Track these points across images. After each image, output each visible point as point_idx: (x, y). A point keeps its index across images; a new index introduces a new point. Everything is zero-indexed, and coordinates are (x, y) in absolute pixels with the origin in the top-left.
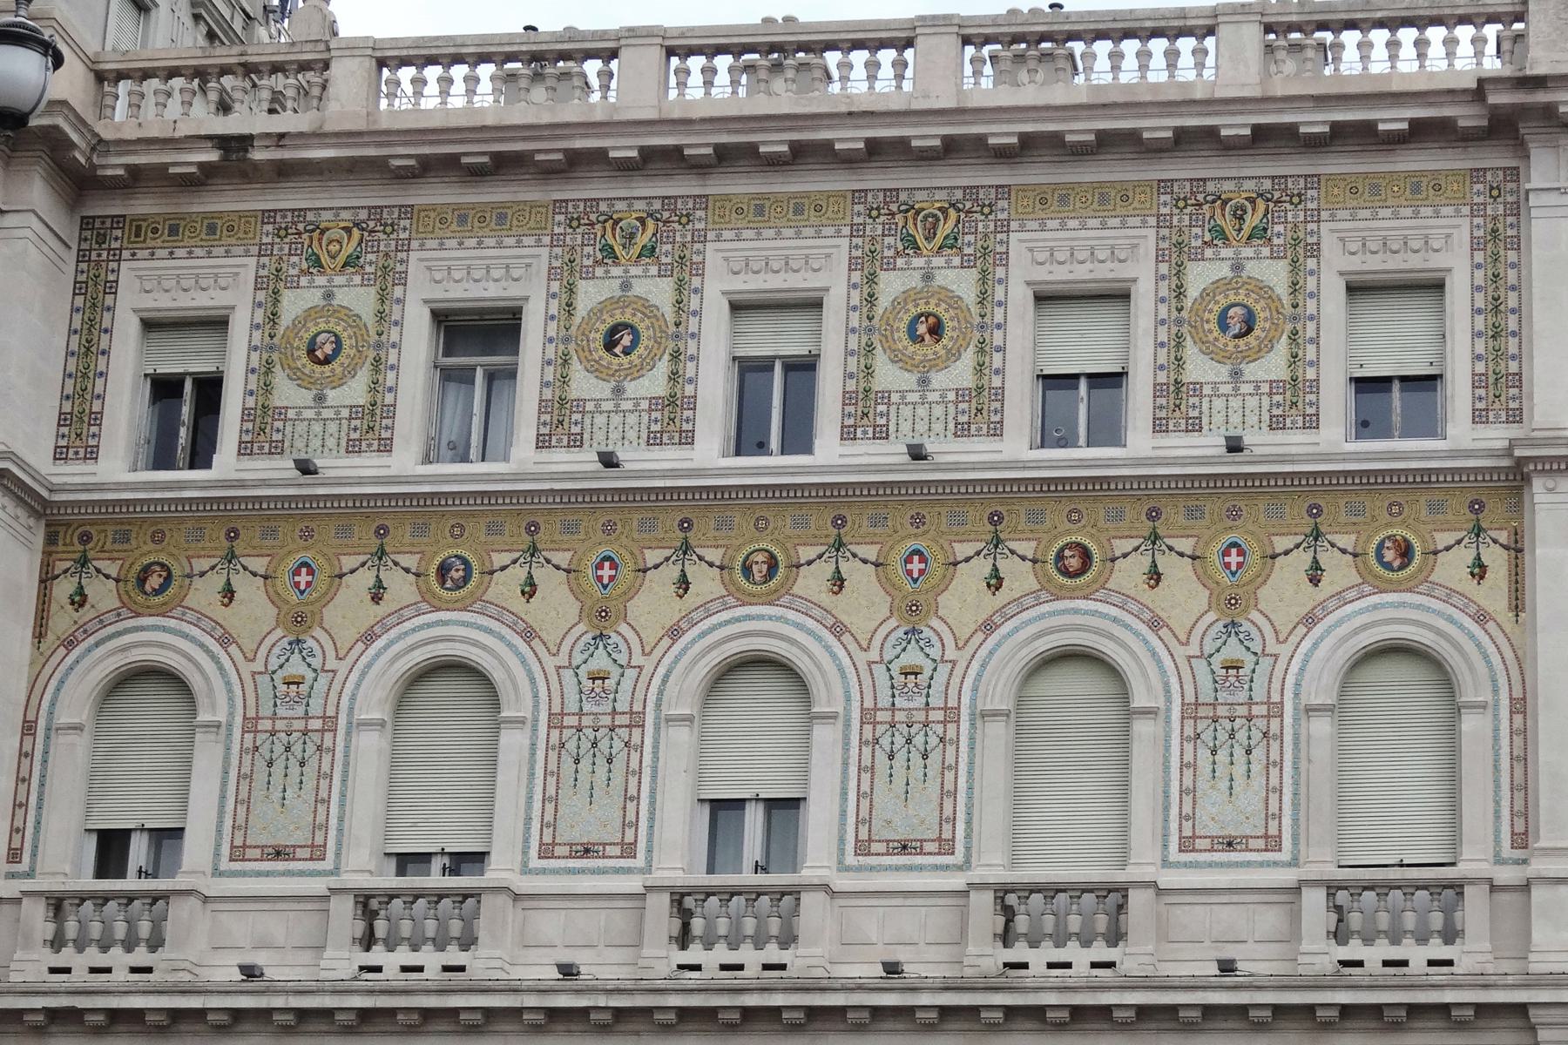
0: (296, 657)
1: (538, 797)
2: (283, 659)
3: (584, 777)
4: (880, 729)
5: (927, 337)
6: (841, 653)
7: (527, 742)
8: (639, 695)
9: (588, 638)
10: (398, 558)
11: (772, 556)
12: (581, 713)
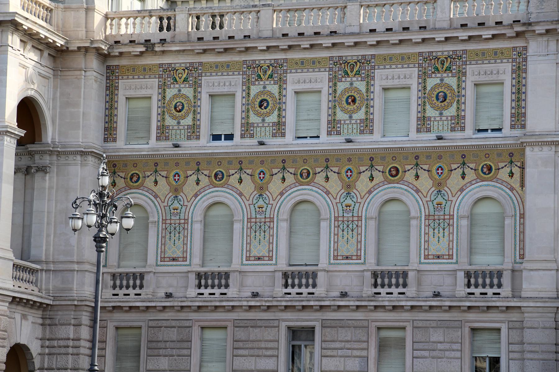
7: (241, 227)
8: (272, 213)
10: (203, 171)
12: (256, 218)
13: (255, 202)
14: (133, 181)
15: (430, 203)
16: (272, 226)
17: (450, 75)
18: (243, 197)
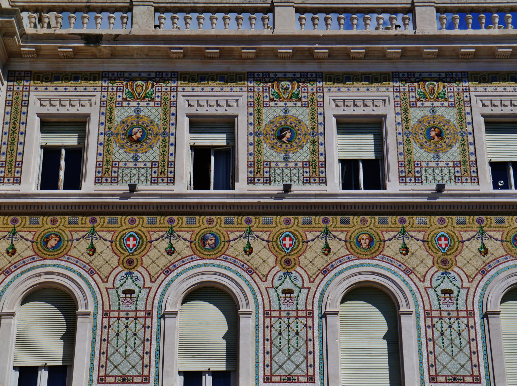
0: (129, 281)
1: (261, 351)
2: (122, 282)
3: (284, 342)
5: (436, 137)
6: (411, 283)
8: (310, 301)
9: (281, 273)
10: (181, 234)
11: (370, 236)
12: (280, 310)
15: (431, 292)
16: (310, 323)
17: (446, 104)
18: (254, 275)
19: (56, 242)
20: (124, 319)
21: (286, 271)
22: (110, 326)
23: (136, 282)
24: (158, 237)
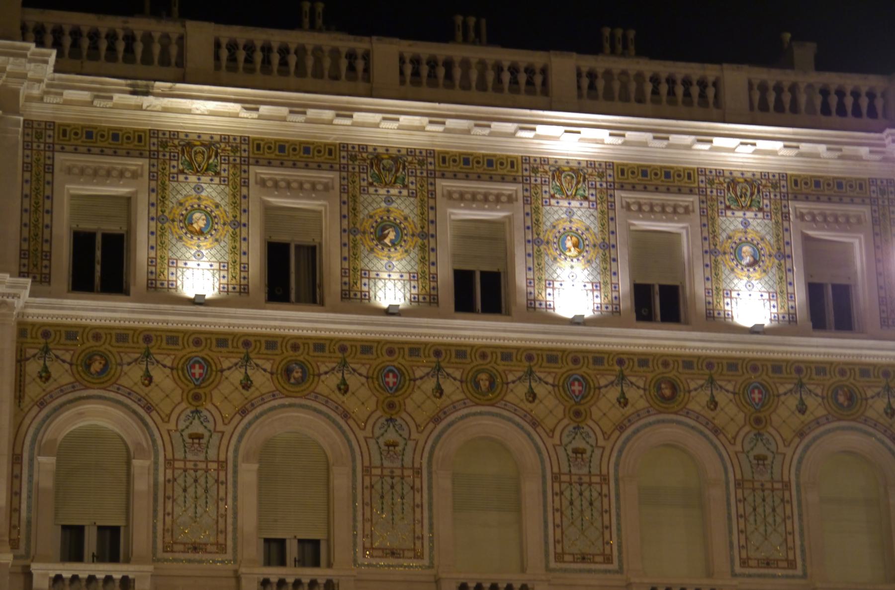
0: (196, 421)
4: (564, 486)
13: (378, 432)
14: (92, 369)
19: (101, 366)
20: (192, 472)
21: (389, 417)
22: (175, 480)
23: (205, 424)
24: (231, 365)
